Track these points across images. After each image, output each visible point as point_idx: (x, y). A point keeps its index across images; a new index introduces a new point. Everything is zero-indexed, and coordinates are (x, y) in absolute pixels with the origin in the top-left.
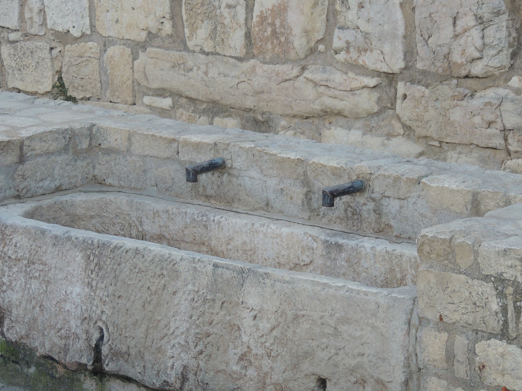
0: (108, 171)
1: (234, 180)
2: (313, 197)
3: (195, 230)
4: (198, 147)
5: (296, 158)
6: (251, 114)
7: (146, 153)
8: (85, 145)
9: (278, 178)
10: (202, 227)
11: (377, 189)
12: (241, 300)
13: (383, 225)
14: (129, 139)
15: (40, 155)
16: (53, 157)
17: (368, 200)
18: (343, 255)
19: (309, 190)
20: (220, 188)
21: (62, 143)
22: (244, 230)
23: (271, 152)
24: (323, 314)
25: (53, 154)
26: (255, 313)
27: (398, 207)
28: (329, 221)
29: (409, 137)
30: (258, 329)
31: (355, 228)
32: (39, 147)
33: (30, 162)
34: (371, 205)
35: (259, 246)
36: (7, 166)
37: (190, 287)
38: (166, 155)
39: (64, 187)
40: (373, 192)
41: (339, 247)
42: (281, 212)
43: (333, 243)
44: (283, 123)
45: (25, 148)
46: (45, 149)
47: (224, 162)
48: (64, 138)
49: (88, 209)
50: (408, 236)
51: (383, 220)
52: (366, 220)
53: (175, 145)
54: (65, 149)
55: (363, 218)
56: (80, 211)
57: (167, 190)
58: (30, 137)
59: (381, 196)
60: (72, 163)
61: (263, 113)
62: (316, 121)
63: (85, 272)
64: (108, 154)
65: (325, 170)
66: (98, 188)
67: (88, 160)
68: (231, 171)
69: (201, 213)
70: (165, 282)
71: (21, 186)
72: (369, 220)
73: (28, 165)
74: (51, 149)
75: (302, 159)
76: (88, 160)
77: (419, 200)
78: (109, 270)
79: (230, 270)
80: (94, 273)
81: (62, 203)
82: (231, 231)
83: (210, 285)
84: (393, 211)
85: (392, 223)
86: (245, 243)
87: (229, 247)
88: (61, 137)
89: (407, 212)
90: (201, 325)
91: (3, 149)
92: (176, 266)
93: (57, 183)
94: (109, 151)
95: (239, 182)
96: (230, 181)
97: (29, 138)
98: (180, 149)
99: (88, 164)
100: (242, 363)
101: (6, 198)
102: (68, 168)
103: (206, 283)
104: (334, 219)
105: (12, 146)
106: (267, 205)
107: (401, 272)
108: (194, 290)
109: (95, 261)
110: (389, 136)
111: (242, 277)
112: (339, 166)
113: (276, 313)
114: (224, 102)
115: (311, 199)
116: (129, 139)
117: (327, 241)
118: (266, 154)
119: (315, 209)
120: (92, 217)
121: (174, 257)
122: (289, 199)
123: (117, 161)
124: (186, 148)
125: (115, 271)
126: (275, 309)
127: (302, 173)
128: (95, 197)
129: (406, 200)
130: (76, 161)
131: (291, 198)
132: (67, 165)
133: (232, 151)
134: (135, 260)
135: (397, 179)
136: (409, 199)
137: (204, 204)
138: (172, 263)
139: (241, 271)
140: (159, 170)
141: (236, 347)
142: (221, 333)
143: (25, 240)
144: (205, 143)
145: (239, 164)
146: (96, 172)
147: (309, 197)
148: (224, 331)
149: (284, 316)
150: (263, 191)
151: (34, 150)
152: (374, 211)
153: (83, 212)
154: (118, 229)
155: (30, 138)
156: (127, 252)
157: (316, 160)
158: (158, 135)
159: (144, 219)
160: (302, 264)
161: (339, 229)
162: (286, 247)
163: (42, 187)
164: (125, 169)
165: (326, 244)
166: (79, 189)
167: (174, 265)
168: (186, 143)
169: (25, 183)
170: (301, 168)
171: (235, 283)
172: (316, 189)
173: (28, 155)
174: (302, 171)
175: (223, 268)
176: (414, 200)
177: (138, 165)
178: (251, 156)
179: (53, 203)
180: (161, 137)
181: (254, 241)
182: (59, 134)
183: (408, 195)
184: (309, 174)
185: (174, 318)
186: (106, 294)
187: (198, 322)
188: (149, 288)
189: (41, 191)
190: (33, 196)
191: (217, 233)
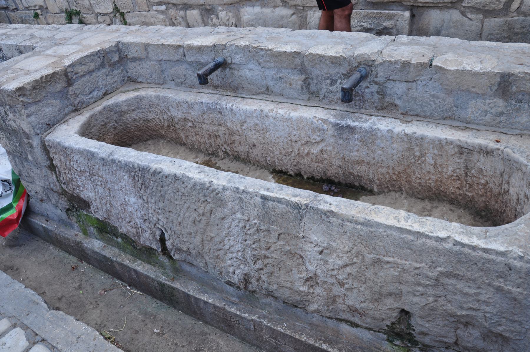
0: (137, 74)
1: (236, 72)
2: (311, 82)
3: (212, 115)
4: (200, 49)
5: (293, 51)
6: (204, 7)
7: (161, 58)
8: (116, 58)
9: (276, 69)
10: (217, 113)
11: (381, 74)
12: (301, 235)
13: (386, 104)
14: (146, 50)
15: (84, 76)
16: (94, 74)
17: (371, 83)
18: (356, 136)
19: (307, 76)
20: (225, 80)
21: (99, 61)
22: (254, 115)
23: (266, 48)
24: (418, 265)
25: (93, 71)
26: (321, 249)
27: (405, 89)
28: (330, 102)
29: (285, 6)
30: (326, 263)
31: (357, 107)
32: (81, 69)
33: (77, 83)
34: (375, 88)
35: (270, 127)
36: (59, 92)
37: (239, 215)
38: (177, 57)
39: (109, 92)
40: (376, 77)
41: (352, 129)
42: (280, 95)
43: (344, 126)
44: (220, 8)
45: (69, 74)
46: (86, 70)
47: (225, 60)
48: (99, 57)
49: (129, 105)
50: (416, 113)
51: (387, 100)
52: (369, 100)
53: (181, 50)
54: (102, 65)
55: (366, 99)
56: (124, 108)
57: (182, 83)
58: (71, 65)
59: (385, 79)
60: (110, 73)
61: (209, 5)
62: (236, 5)
63: (135, 188)
64: (134, 62)
65: (324, 60)
66: (133, 86)
67: (122, 68)
68: (232, 66)
69: (214, 102)
70: (211, 208)
71: (76, 102)
72: (372, 100)
73: (77, 86)
74: (91, 68)
75: (298, 51)
76: (122, 68)
77: (430, 82)
78: (154, 190)
79: (283, 204)
80: (142, 190)
81: (109, 106)
82: (243, 117)
83: (261, 217)
84: (399, 92)
85: (397, 102)
86: (256, 125)
87: (243, 128)
88: (96, 57)
89: (415, 94)
90: (258, 249)
91: (50, 81)
92: (220, 195)
93: (103, 91)
94: (134, 59)
95: (240, 74)
96: (233, 74)
97: (70, 66)
98: (186, 53)
99: (122, 71)
100: (308, 283)
101: (66, 115)
102: (108, 78)
103: (256, 214)
104: (335, 100)
105: (58, 76)
106: (268, 90)
107: (420, 151)
108: (244, 220)
109: (140, 181)
110: (275, 7)
111: (300, 212)
112: (338, 55)
113: (349, 253)
114: (190, 3)
115: (309, 84)
116: (146, 50)
117: (338, 124)
118: (262, 50)
119: (314, 92)
120: (133, 110)
121: (216, 187)
122: (288, 86)
123: (141, 66)
124: (191, 51)
125: (160, 192)
126: (346, 249)
127: (299, 63)
128: (132, 95)
129: (415, 83)
130: (113, 71)
131: (291, 84)
132: (107, 76)
133: (230, 49)
134: (176, 185)
135: (406, 65)
136: (419, 82)
137: (213, 92)
138: (215, 192)
139: (297, 207)
140: (173, 69)
141: (301, 272)
142: (282, 259)
143: (82, 159)
144: (206, 46)
145: (238, 60)
146: (129, 75)
147: (307, 83)
148: (285, 257)
149: (360, 257)
150: (263, 80)
151: (78, 73)
152: (378, 93)
153: (126, 108)
154: (154, 115)
155: (72, 65)
156: (166, 177)
157: (312, 51)
158: (166, 43)
159: (170, 108)
160: (314, 141)
161: (341, 109)
162: (296, 129)
163: (92, 98)
165: (337, 127)
166: (120, 90)
167: (217, 194)
168: (190, 48)
169: (78, 100)
170: (298, 59)
171: (291, 217)
172: (314, 75)
173: (74, 78)
174: (300, 61)
175: (274, 201)
176: (424, 83)
178: (248, 53)
179: (103, 108)
180: (169, 45)
181: (265, 124)
182: (94, 55)
183: (418, 78)
184: (306, 64)
185: (227, 239)
186: (157, 207)
187: (254, 246)
188: (195, 210)
189: (93, 100)
190: (88, 106)
191: (231, 117)
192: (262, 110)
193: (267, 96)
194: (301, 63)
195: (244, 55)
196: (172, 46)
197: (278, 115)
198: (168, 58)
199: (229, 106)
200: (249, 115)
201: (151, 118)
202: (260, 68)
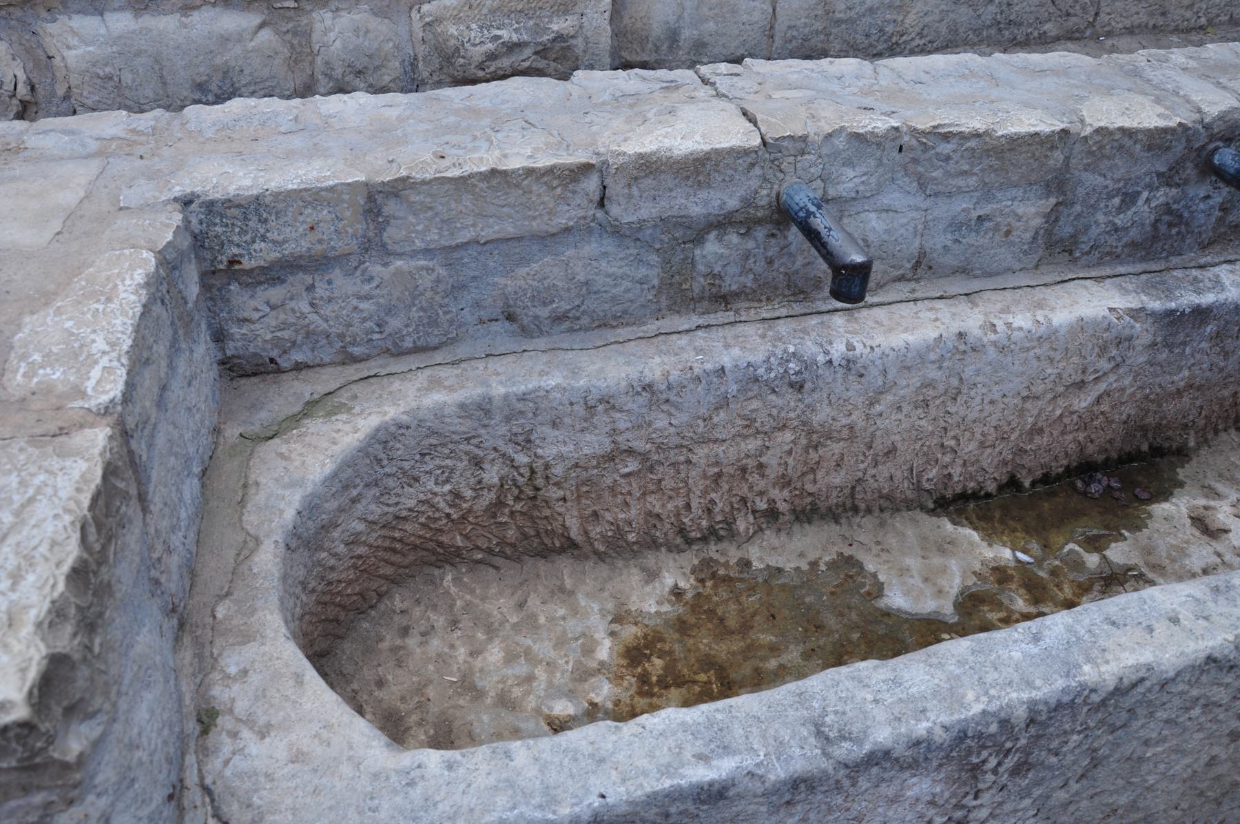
3: (755, 404)
7: (465, 236)
38: (562, 221)
118: (947, 137)
140: (522, 271)
145: (851, 185)
164: (364, 305)
168: (649, 167)
177: (426, 281)
180: (529, 172)
192: (961, 335)
193: (912, 285)
194: (1051, 161)
195: (880, 164)
196: (550, 171)
197: (1016, 333)
198: (510, 229)
199: (838, 350)
200: (909, 361)
201: (411, 503)
202: (919, 200)
